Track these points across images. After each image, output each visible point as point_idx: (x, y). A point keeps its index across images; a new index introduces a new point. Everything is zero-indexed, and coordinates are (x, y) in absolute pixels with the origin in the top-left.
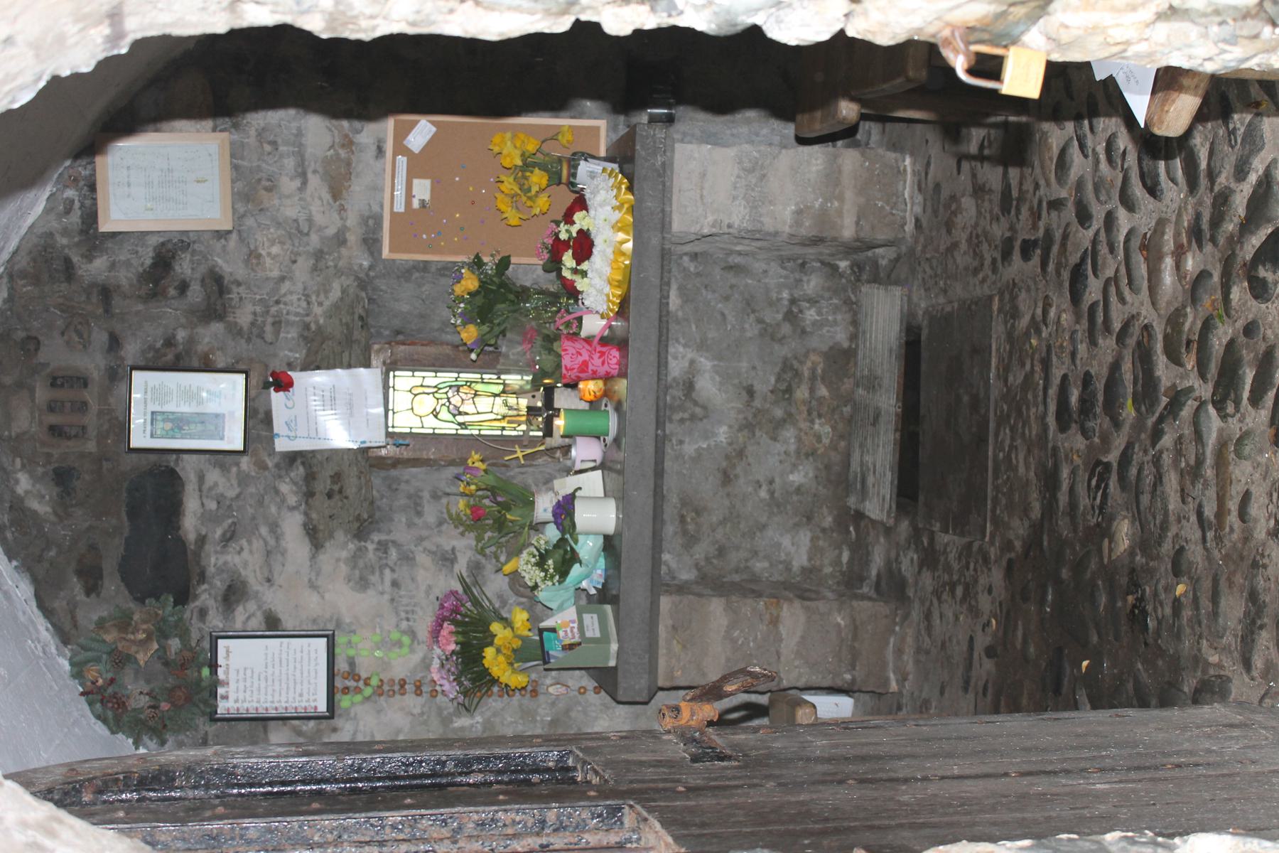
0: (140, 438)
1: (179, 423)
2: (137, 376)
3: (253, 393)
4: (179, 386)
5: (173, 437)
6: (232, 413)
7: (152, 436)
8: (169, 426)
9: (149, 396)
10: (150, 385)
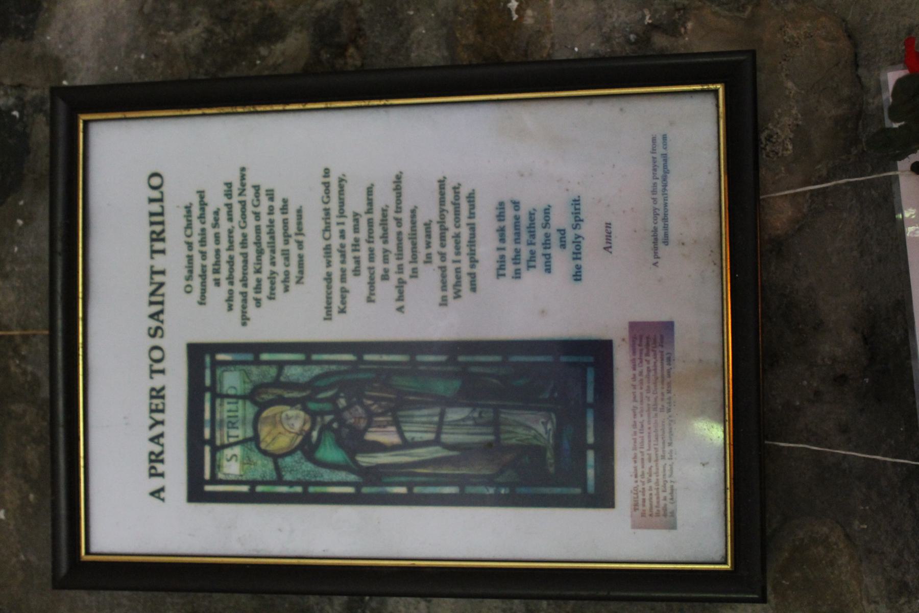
0: (135, 507)
1: (328, 407)
2: (124, 156)
3: (781, 205)
4: (333, 186)
5: (308, 495)
6: (653, 337)
7: (197, 492)
8: (288, 425)
9: (174, 261)
10: (177, 197)
